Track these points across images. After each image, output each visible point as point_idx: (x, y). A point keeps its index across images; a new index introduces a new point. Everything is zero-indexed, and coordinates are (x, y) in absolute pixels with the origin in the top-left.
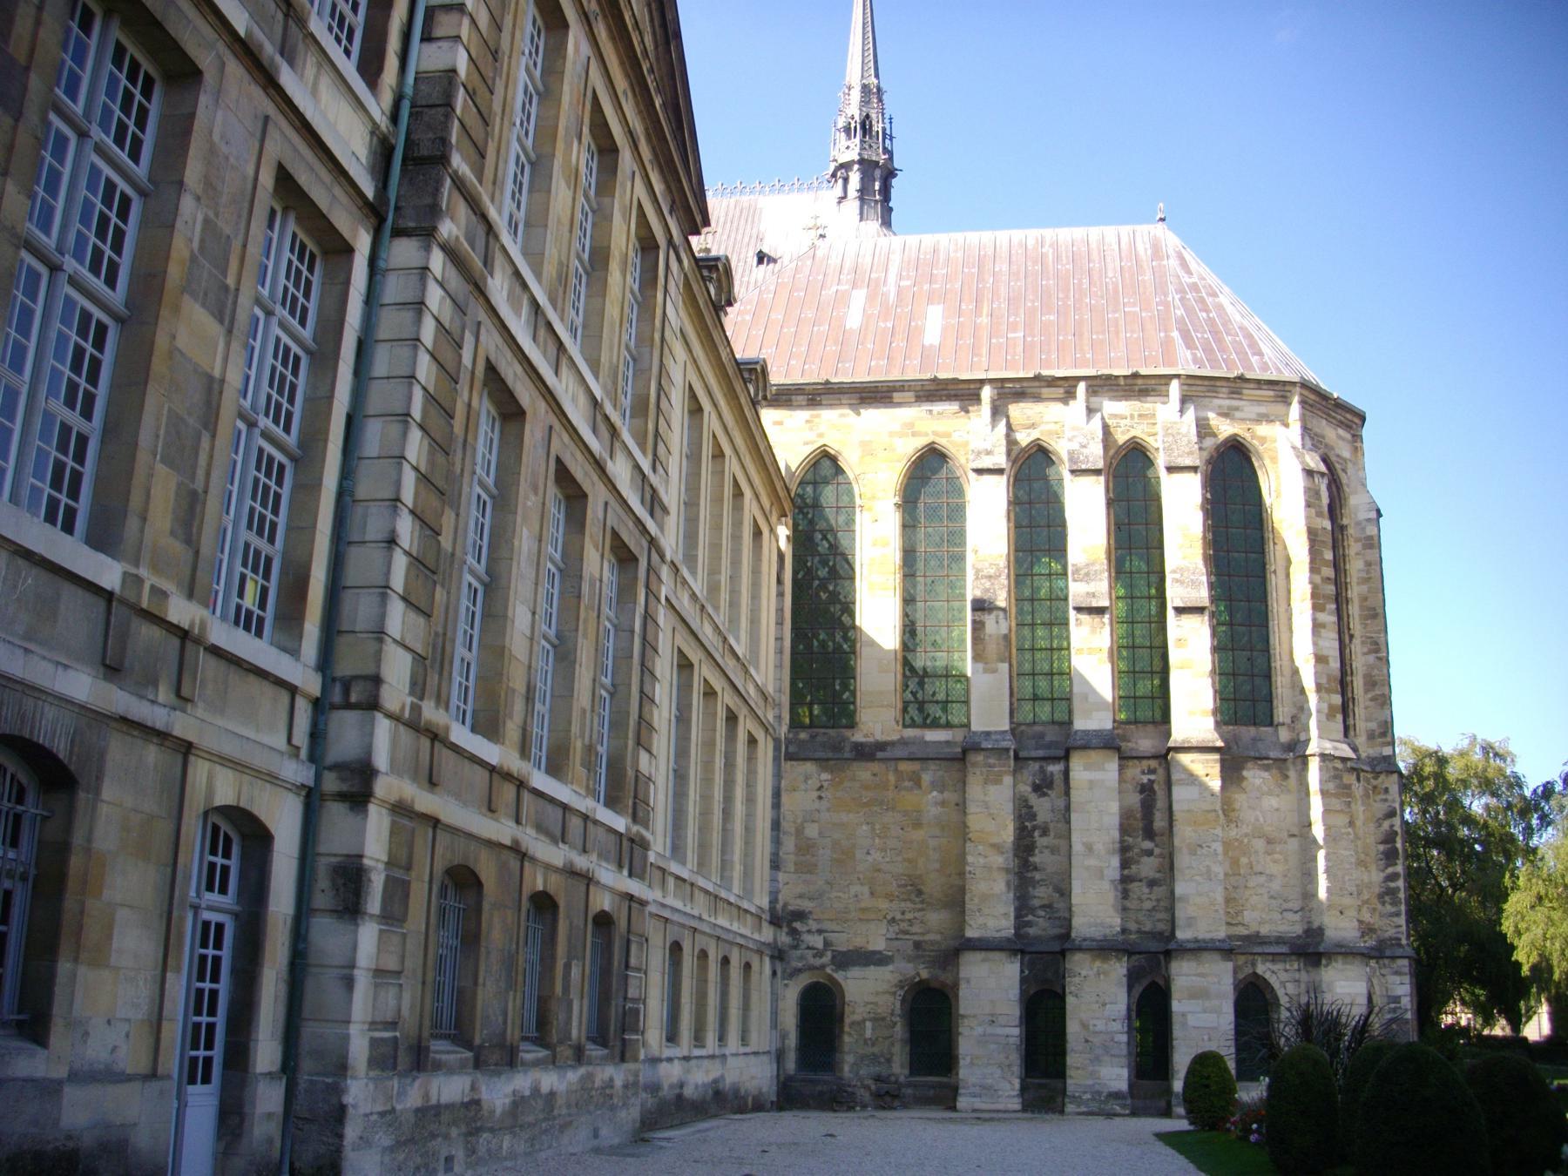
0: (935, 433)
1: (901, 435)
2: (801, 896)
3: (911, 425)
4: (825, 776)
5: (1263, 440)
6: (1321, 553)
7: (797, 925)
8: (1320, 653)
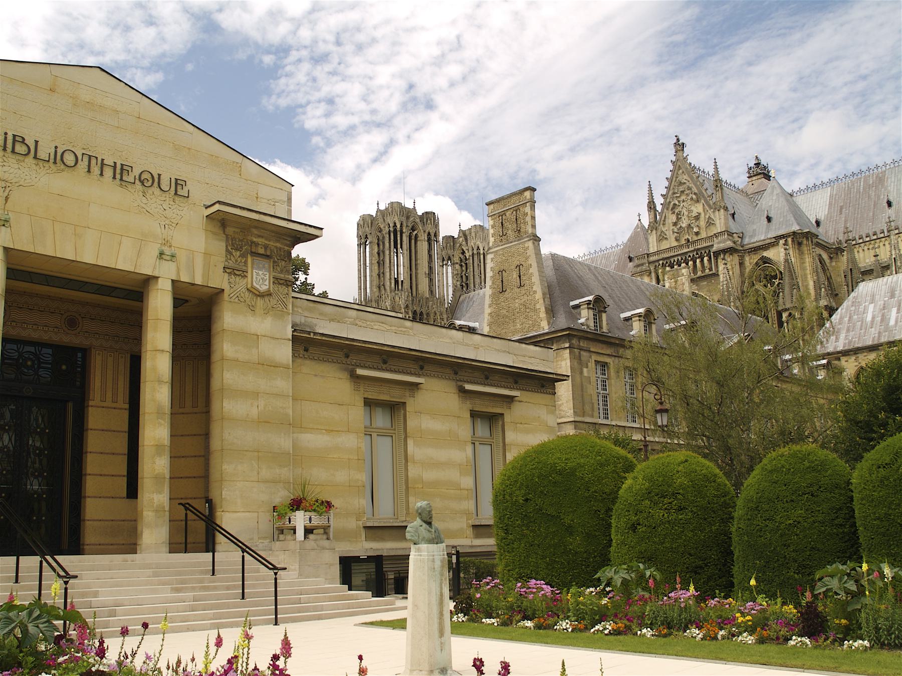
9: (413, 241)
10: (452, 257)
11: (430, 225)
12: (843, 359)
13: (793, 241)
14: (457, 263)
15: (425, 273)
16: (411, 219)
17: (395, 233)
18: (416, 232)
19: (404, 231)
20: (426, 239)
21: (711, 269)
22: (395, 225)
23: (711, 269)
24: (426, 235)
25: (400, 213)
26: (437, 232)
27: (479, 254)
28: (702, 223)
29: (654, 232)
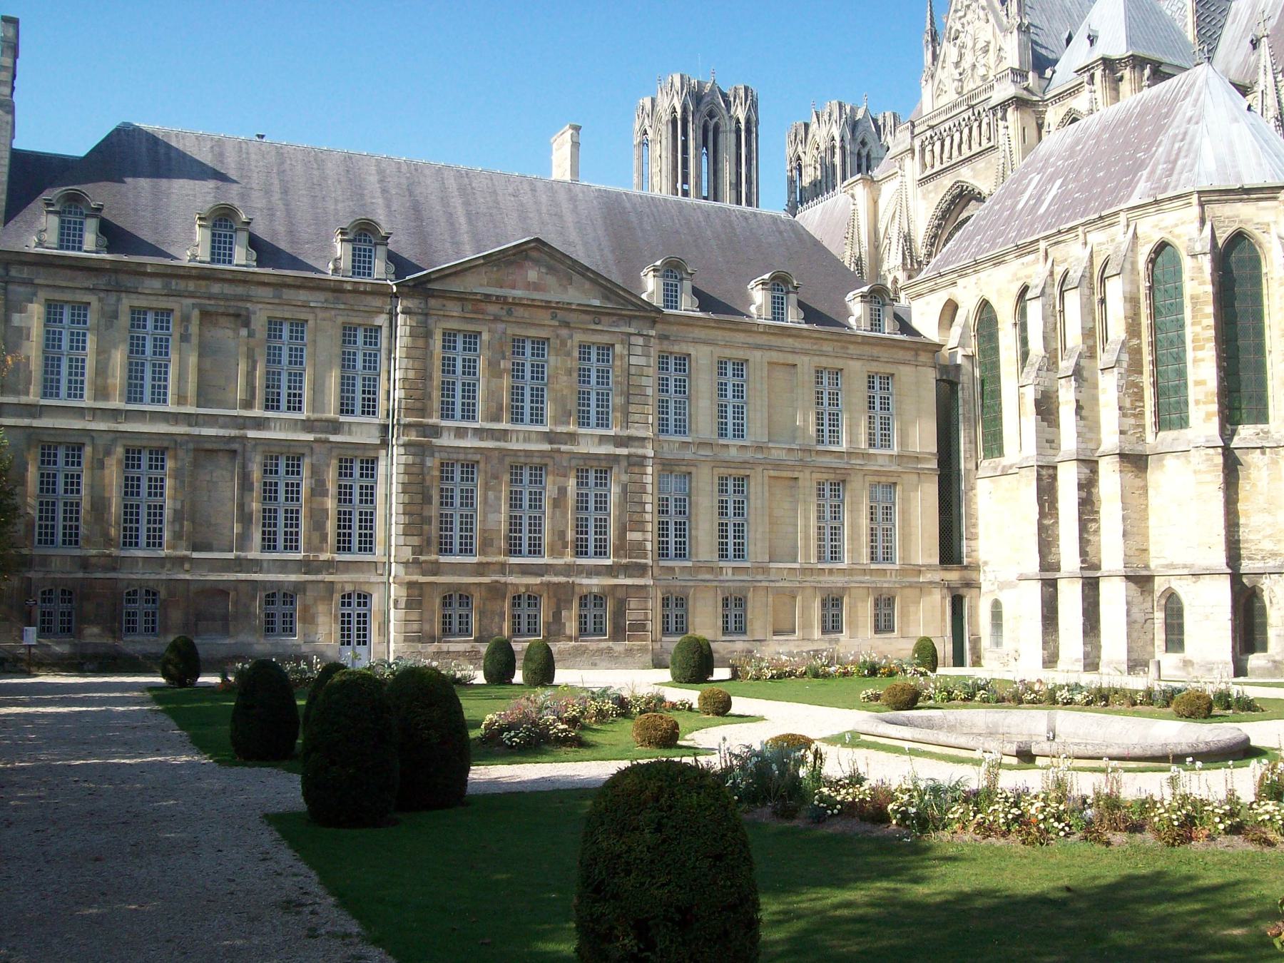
0: (1028, 277)
3: (1015, 274)
5: (1178, 237)
6: (1201, 310)
8: (1199, 379)
9: (711, 135)
10: (802, 155)
13: (1104, 76)
14: (810, 165)
21: (989, 139)
22: (674, 111)
23: (989, 139)
27: (834, 147)
28: (992, 56)
29: (930, 81)
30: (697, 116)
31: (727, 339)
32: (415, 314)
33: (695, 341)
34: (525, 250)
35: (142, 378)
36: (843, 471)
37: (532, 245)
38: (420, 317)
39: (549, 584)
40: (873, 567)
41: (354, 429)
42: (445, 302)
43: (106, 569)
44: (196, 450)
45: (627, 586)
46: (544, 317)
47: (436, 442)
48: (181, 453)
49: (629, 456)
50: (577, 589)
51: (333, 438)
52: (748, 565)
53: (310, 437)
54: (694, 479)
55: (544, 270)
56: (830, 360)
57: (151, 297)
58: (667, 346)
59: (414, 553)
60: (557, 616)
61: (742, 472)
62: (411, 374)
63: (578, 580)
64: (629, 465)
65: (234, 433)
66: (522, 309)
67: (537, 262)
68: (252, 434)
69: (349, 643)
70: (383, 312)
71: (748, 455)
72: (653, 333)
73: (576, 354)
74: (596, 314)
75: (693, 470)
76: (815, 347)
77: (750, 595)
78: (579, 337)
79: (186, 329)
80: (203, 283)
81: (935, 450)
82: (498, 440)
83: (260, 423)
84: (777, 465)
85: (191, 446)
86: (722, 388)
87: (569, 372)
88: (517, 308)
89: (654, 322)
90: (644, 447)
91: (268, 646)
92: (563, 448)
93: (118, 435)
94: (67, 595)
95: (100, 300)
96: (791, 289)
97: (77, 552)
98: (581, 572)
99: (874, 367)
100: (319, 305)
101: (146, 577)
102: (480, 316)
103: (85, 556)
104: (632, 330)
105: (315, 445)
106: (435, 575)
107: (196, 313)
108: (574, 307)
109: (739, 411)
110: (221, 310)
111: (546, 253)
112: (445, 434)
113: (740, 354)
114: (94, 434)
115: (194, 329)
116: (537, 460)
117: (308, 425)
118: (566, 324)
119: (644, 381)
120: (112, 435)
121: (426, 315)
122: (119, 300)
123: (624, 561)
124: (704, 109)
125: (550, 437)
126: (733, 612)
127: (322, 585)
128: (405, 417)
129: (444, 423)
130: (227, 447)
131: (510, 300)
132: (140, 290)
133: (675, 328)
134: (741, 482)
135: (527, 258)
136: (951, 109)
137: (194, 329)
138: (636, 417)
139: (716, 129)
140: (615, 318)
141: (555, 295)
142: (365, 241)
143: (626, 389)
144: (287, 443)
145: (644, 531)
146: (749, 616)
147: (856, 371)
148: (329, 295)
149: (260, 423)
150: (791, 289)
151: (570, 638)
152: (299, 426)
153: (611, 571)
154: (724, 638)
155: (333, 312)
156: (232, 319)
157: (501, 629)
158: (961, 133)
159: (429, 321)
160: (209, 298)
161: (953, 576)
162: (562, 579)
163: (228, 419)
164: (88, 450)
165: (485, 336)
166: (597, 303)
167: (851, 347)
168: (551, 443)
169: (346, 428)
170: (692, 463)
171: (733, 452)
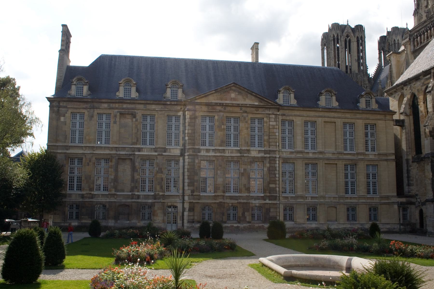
1: (422, 86)
2: (417, 191)
3: (423, 83)
4: (418, 165)
7: (417, 197)
9: (348, 43)
11: (358, 33)
12: (405, 88)
14: (387, 51)
15: (356, 60)
16: (346, 31)
17: (336, 40)
18: (349, 38)
19: (339, 38)
20: (356, 40)
22: (334, 36)
24: (356, 38)
25: (337, 29)
26: (363, 37)
27: (395, 44)
30: (342, 37)
31: (308, 114)
32: (191, 111)
33: (295, 116)
34: (230, 87)
35: (102, 136)
36: (355, 161)
37: (232, 85)
38: (193, 112)
39: (240, 203)
40: (368, 196)
41: (171, 150)
42: (202, 106)
43: (89, 198)
44: (118, 159)
45: (270, 203)
46: (237, 109)
47: (198, 154)
48: (114, 160)
49: (270, 157)
50: (251, 204)
51: (164, 154)
52: (317, 196)
53: (156, 154)
54: (295, 165)
55: (237, 93)
56: (349, 120)
57: (104, 110)
58: (284, 118)
59: (191, 193)
60: (243, 214)
61: (314, 162)
62: (190, 131)
63: (251, 201)
64: (270, 160)
65: (130, 153)
66: (229, 107)
67: (234, 91)
68: (137, 153)
69: (170, 223)
70: (181, 111)
71: (316, 156)
72: (278, 113)
73: (249, 122)
74: (257, 107)
75: (295, 162)
76: (343, 115)
77: (318, 207)
78: (250, 116)
79: (115, 119)
80: (121, 104)
81: (394, 152)
82: (221, 153)
83: (139, 150)
84: (328, 159)
85: (117, 158)
86: (306, 132)
87: (247, 128)
88: (228, 107)
89: (279, 110)
90: (276, 154)
91: (142, 224)
92: (245, 155)
93: (94, 155)
94: (78, 207)
95: (88, 111)
96: (333, 95)
97: (80, 192)
98: (252, 199)
99: (367, 121)
100: (159, 110)
101: (102, 201)
102: (214, 111)
103: (83, 194)
104: (270, 113)
105: (158, 156)
106: (199, 200)
107: (118, 114)
108: (248, 106)
109: (313, 140)
110: (127, 113)
111: (237, 87)
112: (202, 152)
113: (313, 119)
114: (86, 154)
115: (118, 119)
116: (236, 160)
117: (155, 150)
118: (246, 112)
119: (275, 130)
120: (91, 155)
121: (195, 111)
122: (94, 111)
123: (268, 194)
124: (345, 34)
125: (240, 151)
126: (351, 213)
127: (160, 203)
128: (188, 146)
129: (201, 148)
130: (128, 158)
131: (225, 104)
132: (100, 108)
133: (287, 111)
134: (315, 165)
135: (231, 90)
136: (423, 24)
137: (118, 119)
138: (273, 144)
139: (350, 41)
140: (264, 109)
141: (241, 101)
142: (175, 87)
143: (268, 134)
144: (149, 156)
145: (276, 184)
146: (318, 215)
147: (360, 124)
148: (163, 106)
149: (139, 150)
150: (333, 95)
151: (249, 222)
152: (153, 150)
153: (263, 198)
154: (308, 223)
155: (164, 112)
156: (130, 115)
157: (223, 218)
158: (427, 32)
159: (196, 113)
160: (123, 109)
161: (404, 200)
162: (245, 201)
163: (129, 149)
164: (84, 159)
165: (216, 117)
166: (257, 104)
167: (358, 114)
168: (240, 153)
169: (169, 150)
170: (296, 159)
171: (311, 155)
